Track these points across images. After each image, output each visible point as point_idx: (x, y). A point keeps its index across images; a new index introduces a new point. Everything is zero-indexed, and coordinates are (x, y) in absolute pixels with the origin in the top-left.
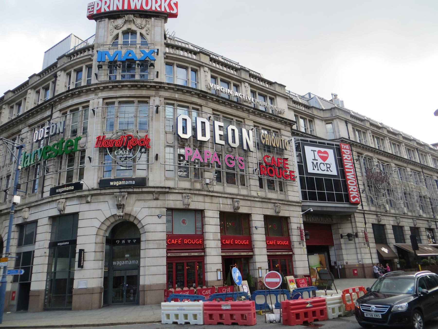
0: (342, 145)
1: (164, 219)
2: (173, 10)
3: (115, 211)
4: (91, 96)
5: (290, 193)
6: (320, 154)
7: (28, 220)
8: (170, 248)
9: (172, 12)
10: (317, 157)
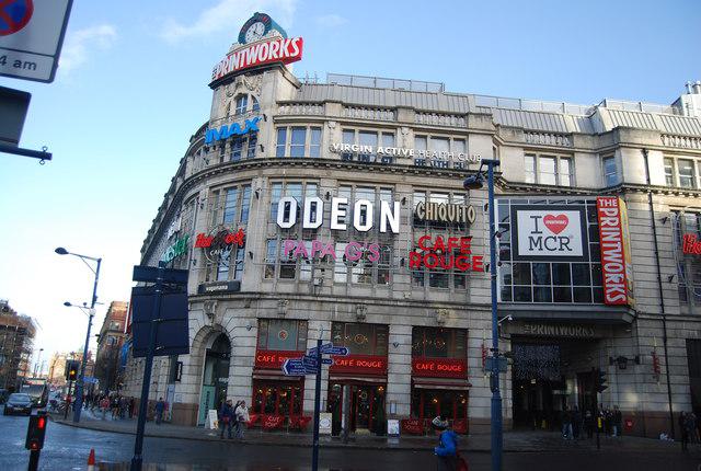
0: (601, 201)
1: (254, 332)
2: (293, 51)
3: (208, 322)
5: (473, 291)
6: (548, 222)
8: (258, 366)
9: (292, 55)
10: (542, 227)
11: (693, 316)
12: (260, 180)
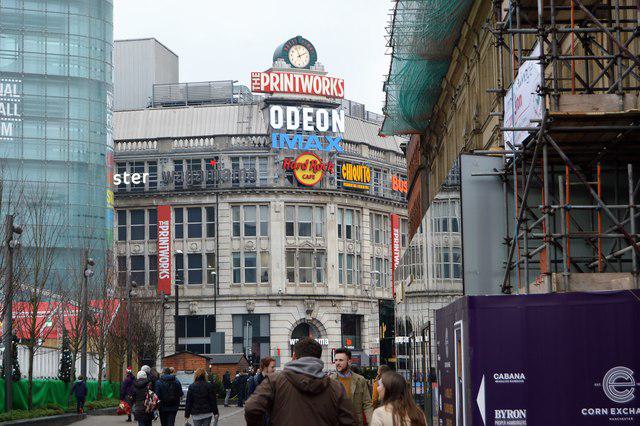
4: (271, 198)
7: (197, 314)
11: (331, 300)
12: (332, 206)
